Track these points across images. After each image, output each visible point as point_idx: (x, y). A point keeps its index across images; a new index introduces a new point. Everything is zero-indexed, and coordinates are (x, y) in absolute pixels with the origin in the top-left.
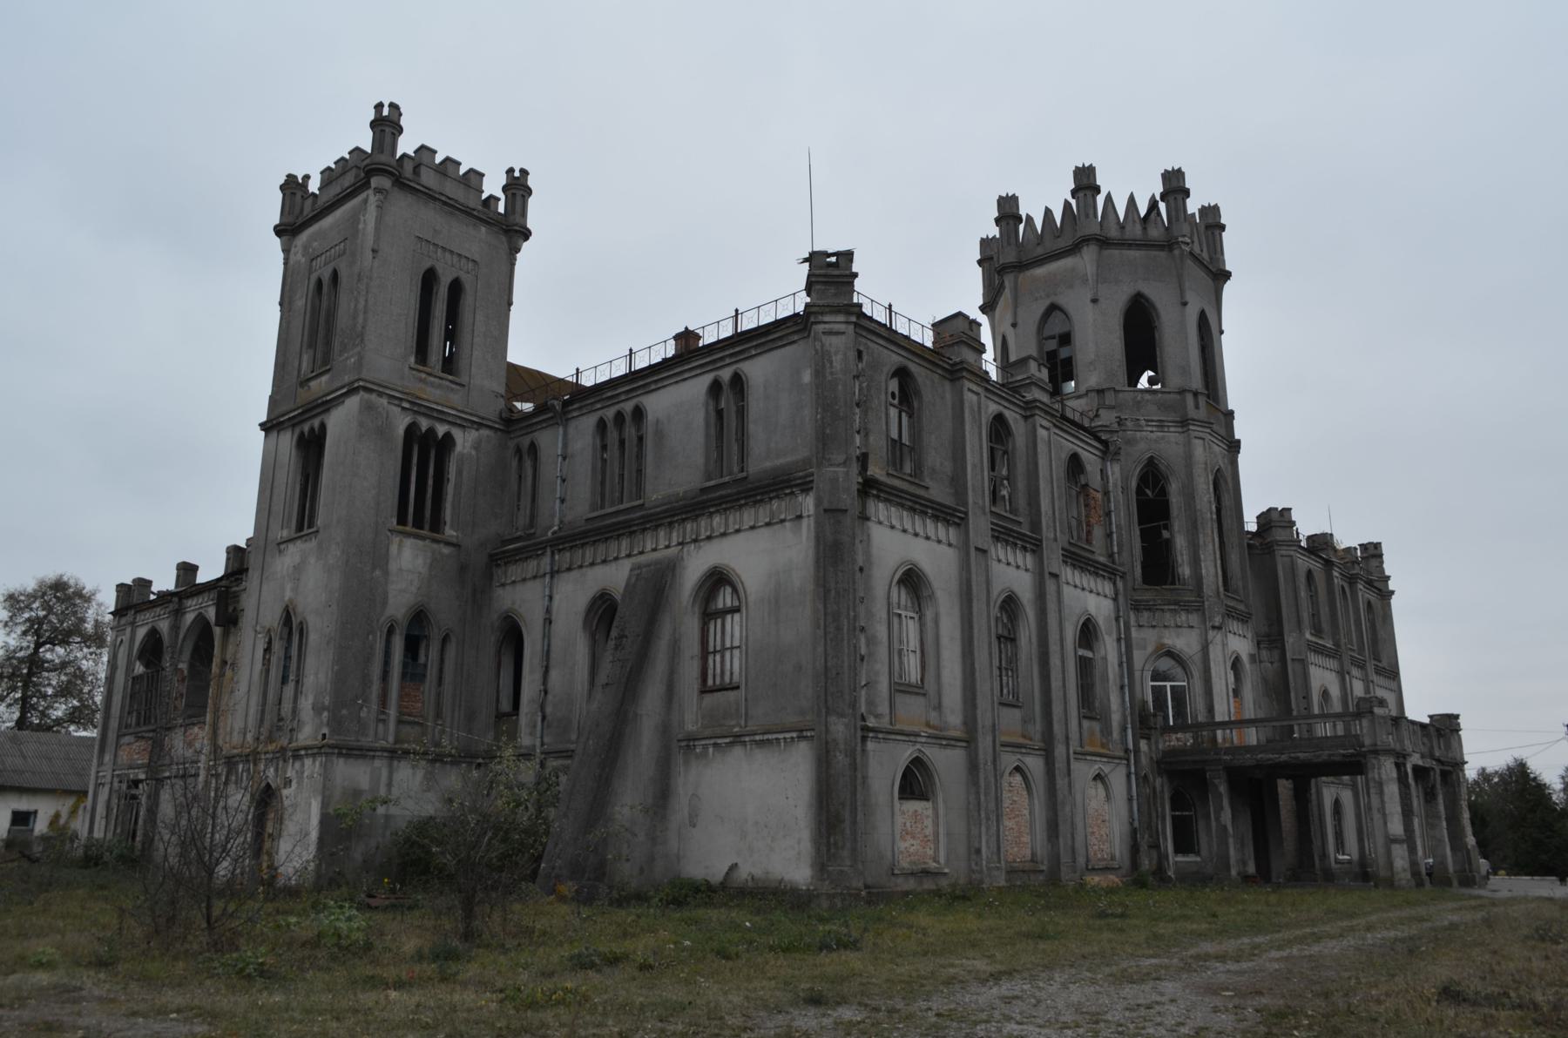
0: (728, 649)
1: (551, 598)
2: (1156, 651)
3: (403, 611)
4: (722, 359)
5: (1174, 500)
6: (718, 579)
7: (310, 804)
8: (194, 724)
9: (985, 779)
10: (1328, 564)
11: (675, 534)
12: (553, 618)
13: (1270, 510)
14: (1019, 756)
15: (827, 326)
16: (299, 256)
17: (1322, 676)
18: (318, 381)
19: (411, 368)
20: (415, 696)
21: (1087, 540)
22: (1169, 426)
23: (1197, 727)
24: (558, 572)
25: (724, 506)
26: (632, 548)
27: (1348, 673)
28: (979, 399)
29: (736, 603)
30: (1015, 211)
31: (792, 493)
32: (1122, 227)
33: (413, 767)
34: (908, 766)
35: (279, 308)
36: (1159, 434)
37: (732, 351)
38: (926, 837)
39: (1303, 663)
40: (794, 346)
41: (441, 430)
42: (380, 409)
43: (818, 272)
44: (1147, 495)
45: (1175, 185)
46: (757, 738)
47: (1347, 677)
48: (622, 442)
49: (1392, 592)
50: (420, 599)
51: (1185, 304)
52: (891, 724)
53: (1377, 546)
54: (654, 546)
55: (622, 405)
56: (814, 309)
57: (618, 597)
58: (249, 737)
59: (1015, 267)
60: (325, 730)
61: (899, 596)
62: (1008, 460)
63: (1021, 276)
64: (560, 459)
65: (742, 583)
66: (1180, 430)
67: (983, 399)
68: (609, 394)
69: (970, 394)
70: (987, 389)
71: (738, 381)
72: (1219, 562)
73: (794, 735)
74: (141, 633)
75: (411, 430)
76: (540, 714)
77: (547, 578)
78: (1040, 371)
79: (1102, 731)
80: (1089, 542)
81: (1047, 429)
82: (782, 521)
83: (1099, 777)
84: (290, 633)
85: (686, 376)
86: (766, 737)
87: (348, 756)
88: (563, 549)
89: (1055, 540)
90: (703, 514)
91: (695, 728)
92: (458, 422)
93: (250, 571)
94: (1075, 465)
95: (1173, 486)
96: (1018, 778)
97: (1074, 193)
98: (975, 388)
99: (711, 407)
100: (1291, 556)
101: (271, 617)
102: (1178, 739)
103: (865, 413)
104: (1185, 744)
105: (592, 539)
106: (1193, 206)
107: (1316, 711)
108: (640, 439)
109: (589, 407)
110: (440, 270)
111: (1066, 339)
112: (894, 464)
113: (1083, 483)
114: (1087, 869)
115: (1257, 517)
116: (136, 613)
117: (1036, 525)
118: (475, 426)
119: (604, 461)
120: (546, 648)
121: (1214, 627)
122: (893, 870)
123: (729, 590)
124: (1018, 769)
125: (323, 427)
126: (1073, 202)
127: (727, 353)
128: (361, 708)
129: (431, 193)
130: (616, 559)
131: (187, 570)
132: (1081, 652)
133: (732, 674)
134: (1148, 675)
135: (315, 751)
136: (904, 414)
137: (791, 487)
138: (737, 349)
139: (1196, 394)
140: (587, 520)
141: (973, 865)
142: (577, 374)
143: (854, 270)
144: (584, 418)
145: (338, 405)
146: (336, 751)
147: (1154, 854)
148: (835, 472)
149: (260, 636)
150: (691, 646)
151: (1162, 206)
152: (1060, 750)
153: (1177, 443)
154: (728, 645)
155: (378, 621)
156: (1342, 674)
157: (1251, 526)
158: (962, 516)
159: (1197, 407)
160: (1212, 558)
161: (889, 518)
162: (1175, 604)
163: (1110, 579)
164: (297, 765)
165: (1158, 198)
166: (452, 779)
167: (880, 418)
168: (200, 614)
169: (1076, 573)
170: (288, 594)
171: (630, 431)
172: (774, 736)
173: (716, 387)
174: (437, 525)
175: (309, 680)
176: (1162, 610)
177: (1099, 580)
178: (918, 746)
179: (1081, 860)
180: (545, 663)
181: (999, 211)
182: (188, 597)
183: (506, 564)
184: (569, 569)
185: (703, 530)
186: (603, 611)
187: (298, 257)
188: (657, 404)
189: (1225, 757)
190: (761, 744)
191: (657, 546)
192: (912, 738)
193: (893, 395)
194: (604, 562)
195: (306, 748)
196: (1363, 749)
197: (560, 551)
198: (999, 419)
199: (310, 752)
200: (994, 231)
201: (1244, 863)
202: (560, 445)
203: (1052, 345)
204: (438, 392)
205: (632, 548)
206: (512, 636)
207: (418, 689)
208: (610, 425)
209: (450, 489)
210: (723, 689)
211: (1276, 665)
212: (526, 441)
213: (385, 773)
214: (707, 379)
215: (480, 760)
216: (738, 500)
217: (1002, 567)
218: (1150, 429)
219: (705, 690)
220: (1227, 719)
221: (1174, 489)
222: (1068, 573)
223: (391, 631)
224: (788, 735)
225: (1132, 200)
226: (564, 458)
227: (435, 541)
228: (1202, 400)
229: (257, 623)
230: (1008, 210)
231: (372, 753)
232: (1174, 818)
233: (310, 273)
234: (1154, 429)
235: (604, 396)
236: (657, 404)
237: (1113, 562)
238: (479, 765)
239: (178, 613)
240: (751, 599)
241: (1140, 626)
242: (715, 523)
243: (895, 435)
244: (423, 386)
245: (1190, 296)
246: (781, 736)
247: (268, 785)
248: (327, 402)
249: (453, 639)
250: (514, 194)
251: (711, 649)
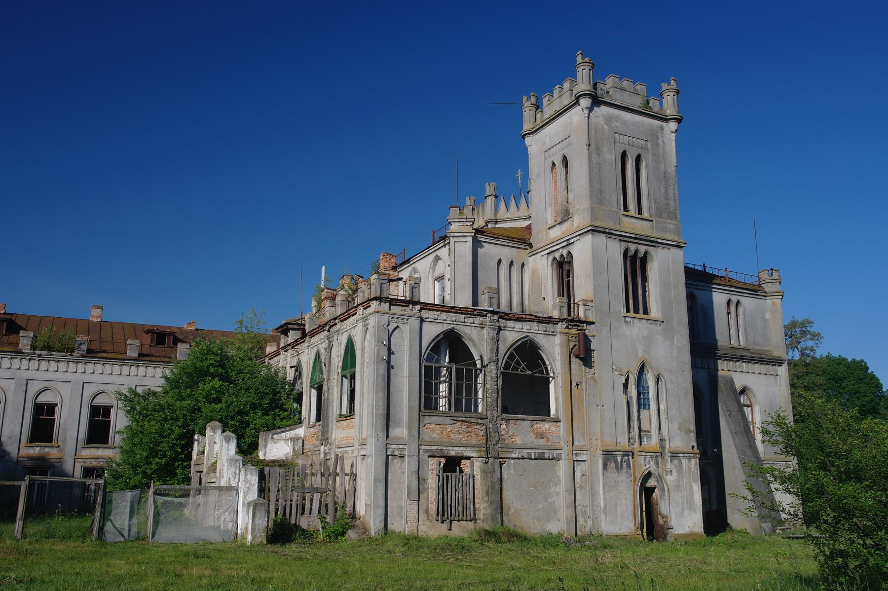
7: (692, 485)
86: (774, 462)
149: (616, 373)
164: (676, 462)
170: (640, 355)
224: (782, 463)
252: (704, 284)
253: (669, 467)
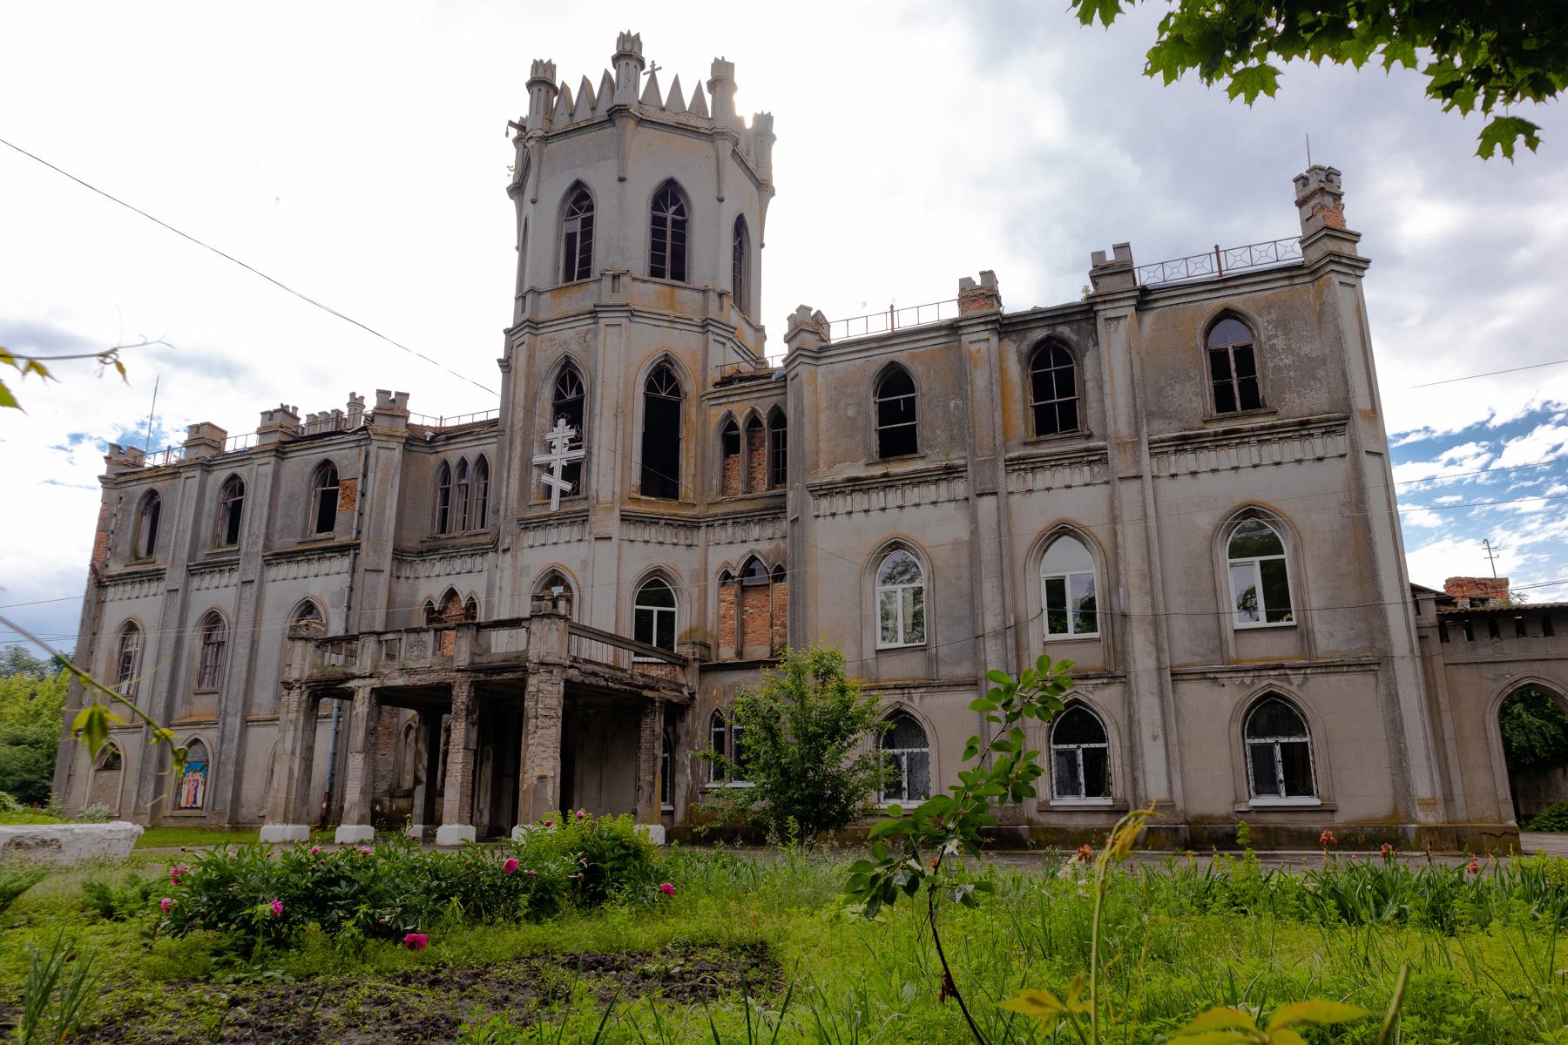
30: (550, 77)
51: (721, 200)
126: (613, 73)
139: (721, 295)
151: (708, 98)
159: (721, 309)
225: (676, 85)
228: (728, 302)
230: (542, 80)
245: (725, 195)
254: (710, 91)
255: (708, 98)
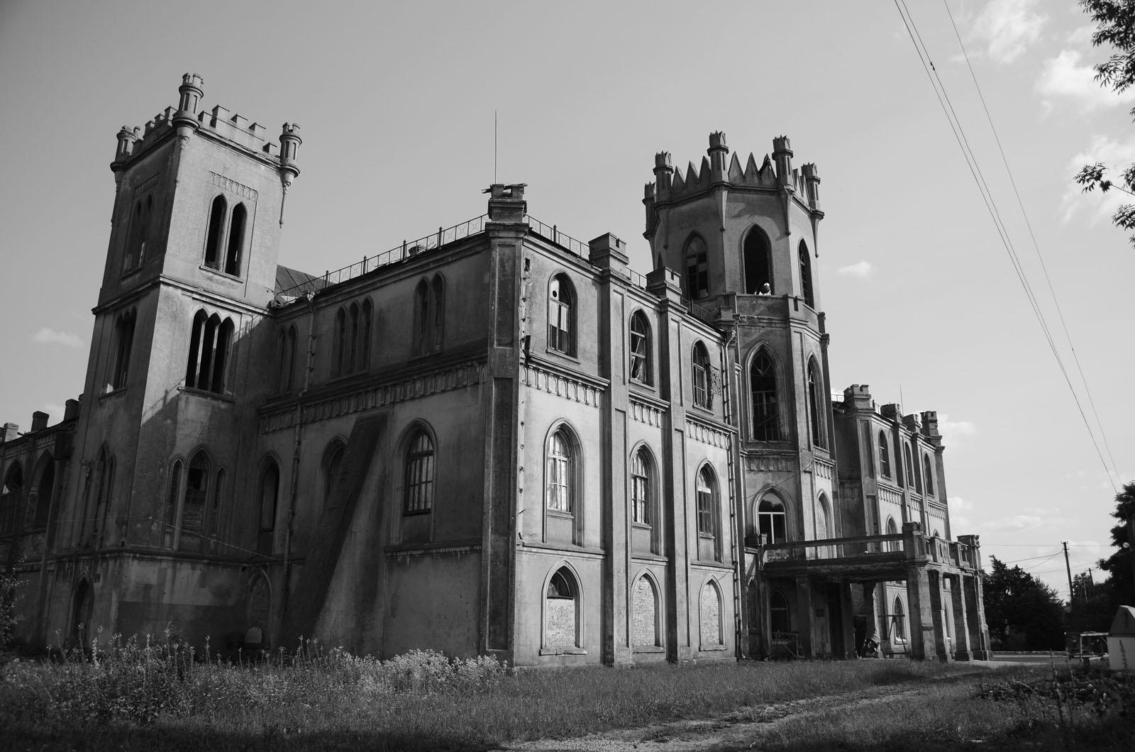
0: (423, 483)
1: (299, 443)
2: (764, 487)
3: (188, 451)
4: (428, 264)
5: (778, 378)
6: (419, 429)
7: (111, 594)
8: (38, 533)
9: (618, 583)
10: (895, 427)
11: (388, 396)
12: (300, 459)
13: (852, 387)
14: (647, 566)
15: (502, 240)
16: (127, 185)
17: (889, 509)
18: (133, 277)
19: (200, 268)
20: (196, 515)
21: (708, 406)
22: (775, 323)
23: (792, 545)
24: (305, 423)
25: (424, 374)
26: (358, 407)
27: (909, 506)
28: (623, 298)
29: (431, 448)
31: (472, 365)
32: (744, 177)
33: (193, 569)
34: (556, 573)
35: (111, 223)
36: (769, 329)
37: (434, 259)
38: (570, 627)
39: (874, 500)
40: (479, 255)
41: (223, 315)
42: (175, 299)
43: (496, 200)
44: (760, 374)
45: (781, 149)
46: (441, 550)
47: (908, 508)
48: (355, 326)
49: (943, 448)
50: (201, 442)
51: (788, 234)
52: (543, 541)
53: (933, 414)
54: (373, 405)
55: (356, 298)
56: (491, 228)
57: (346, 443)
58: (74, 544)
59: (667, 205)
60: (124, 539)
61: (554, 445)
62: (646, 344)
63: (672, 210)
64: (311, 338)
65: (435, 433)
66: (783, 325)
67: (626, 298)
68: (347, 290)
69: (615, 294)
70: (629, 291)
71: (438, 280)
72: (810, 423)
73: (468, 548)
74: (8, 463)
75: (200, 315)
76: (288, 530)
77: (298, 428)
78: (673, 278)
79: (715, 548)
80: (709, 407)
81: (678, 322)
82: (465, 386)
83: (711, 582)
84: (105, 466)
85: (402, 276)
86: (447, 550)
87: (141, 559)
88: (310, 406)
89: (682, 405)
90: (409, 381)
91: (397, 543)
92: (237, 309)
93: (80, 419)
94: (700, 351)
95: (778, 367)
96: (647, 583)
97: (709, 151)
98: (620, 290)
99: (419, 300)
100: (868, 421)
101: (92, 452)
102: (778, 555)
103: (531, 306)
104: (783, 558)
105: (330, 399)
106: (796, 163)
107: (884, 532)
108: (368, 324)
109: (333, 300)
110: (227, 197)
111: (702, 257)
112: (554, 346)
113: (707, 363)
114: (700, 651)
115: (845, 392)
116: (6, 449)
117: (666, 394)
118: (250, 313)
119: (342, 341)
120: (294, 481)
121: (805, 472)
122: (540, 652)
123: (426, 439)
124: (646, 576)
125: (135, 311)
126: (709, 158)
127: (432, 260)
128: (152, 523)
129: (223, 140)
130: (347, 414)
131: (40, 418)
132: (699, 489)
133: (426, 502)
134: (757, 504)
135: (116, 554)
136: (563, 308)
137: (472, 360)
138: (438, 257)
140: (328, 384)
141: (607, 649)
142: (327, 275)
143: (524, 199)
144: (329, 309)
145: (145, 295)
146: (132, 555)
147: (758, 639)
148: (505, 350)
149: (84, 467)
150: (398, 481)
151: (773, 163)
152: (680, 563)
153: (781, 336)
154: (424, 480)
155: (168, 458)
156: (903, 507)
157: (837, 395)
158: (607, 385)
159: (796, 309)
160: (805, 420)
161: (547, 384)
162: (778, 454)
163: (725, 435)
164: (104, 564)
165: (770, 157)
166: (222, 577)
167: (542, 311)
168: (47, 450)
169: (699, 429)
171: (362, 319)
172: (453, 549)
173: (422, 286)
174: (217, 387)
175: (115, 501)
176: (768, 458)
177: (717, 435)
178: (565, 558)
179: (695, 645)
180: (293, 492)
181: (656, 164)
182: (39, 438)
183: (269, 416)
184: (313, 422)
185: (408, 393)
186: (335, 451)
187: (127, 187)
188: (382, 297)
189: (809, 568)
190: (444, 555)
191: (374, 402)
192: (560, 552)
193: (555, 294)
194: (338, 416)
195: (110, 552)
196: (906, 562)
197: (307, 407)
198: (640, 314)
199: (113, 555)
200: (653, 179)
201: (823, 646)
202: (311, 328)
203: (693, 262)
204: (222, 287)
205: (358, 407)
206: (271, 469)
207: (199, 510)
208: (348, 314)
209: (229, 359)
210: (419, 513)
211: (855, 500)
212: (288, 325)
213: (170, 572)
214: (417, 279)
215: (246, 565)
216: (434, 370)
217: (639, 423)
218: (762, 325)
219: (406, 514)
220: (813, 539)
221: (779, 367)
222: (690, 429)
223: (178, 465)
224: (463, 549)
225: (751, 158)
226: (314, 338)
227: (214, 398)
228: (800, 304)
229: (83, 458)
231: (160, 557)
232: (772, 611)
233: (133, 198)
234: (765, 325)
235: (343, 292)
236: (382, 297)
237: (729, 423)
238: (244, 569)
239: (34, 449)
240: (441, 445)
241: (751, 471)
242: (417, 389)
243: (556, 325)
244: (210, 283)
246: (458, 550)
247: (84, 580)
248: (138, 292)
249: (227, 473)
250: (288, 143)
251: (412, 483)
252: (380, 278)
253: (98, 573)
254: (773, 159)
255: (773, 163)
